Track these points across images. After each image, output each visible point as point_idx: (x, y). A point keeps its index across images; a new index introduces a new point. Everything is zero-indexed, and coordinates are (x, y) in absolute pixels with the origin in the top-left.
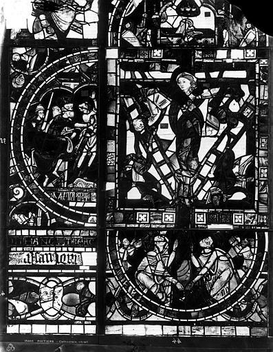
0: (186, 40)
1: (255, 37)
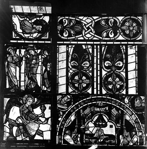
0: (99, 141)
1: (138, 140)
